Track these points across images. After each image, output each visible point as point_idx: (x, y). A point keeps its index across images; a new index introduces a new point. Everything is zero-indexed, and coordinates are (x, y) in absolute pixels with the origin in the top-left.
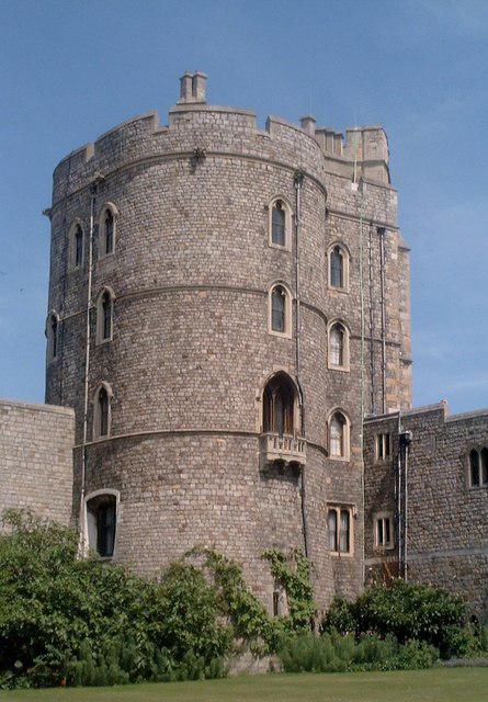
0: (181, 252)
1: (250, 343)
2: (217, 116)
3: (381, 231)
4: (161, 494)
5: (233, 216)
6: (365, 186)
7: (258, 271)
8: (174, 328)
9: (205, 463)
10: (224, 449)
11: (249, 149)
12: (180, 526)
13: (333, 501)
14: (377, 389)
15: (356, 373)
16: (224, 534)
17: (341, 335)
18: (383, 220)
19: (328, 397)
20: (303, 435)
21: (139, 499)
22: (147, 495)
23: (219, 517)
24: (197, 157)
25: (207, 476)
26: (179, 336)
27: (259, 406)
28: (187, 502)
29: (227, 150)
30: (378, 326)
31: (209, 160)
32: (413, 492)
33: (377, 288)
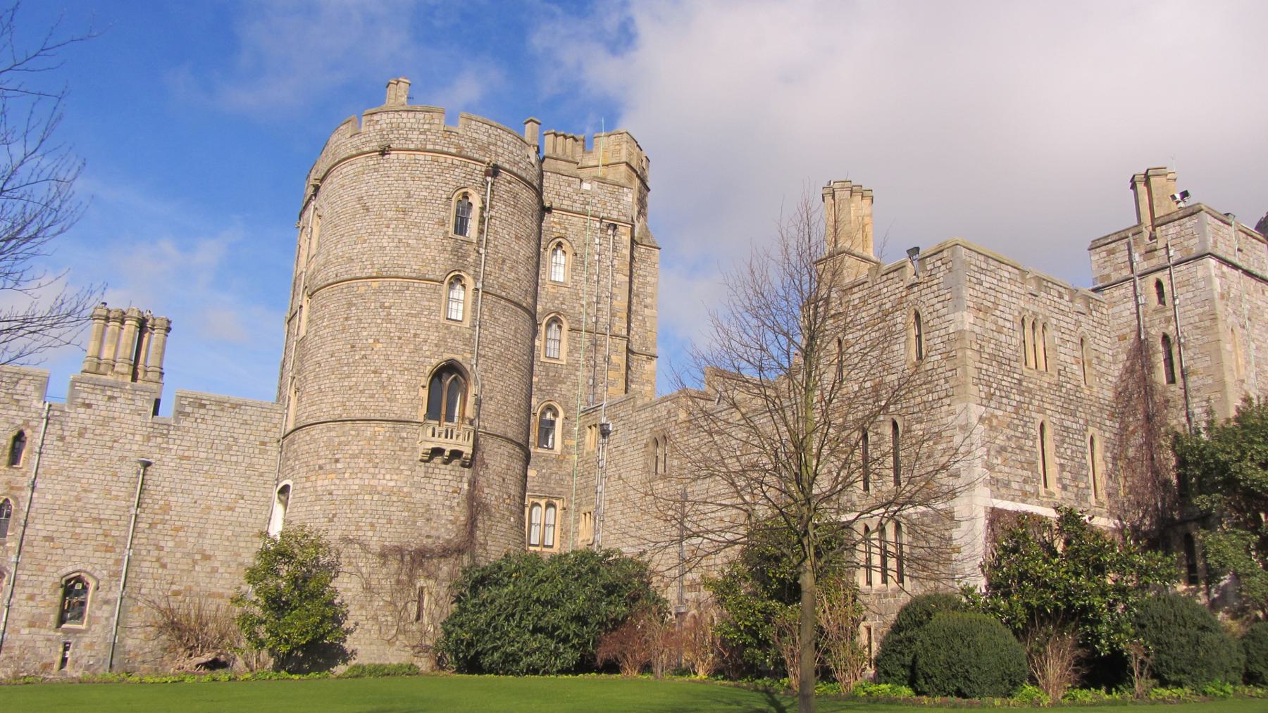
0: (359, 246)
1: (419, 332)
2: (404, 115)
7: (435, 260)
8: (347, 319)
10: (381, 437)
11: (435, 143)
12: (331, 516)
13: (537, 494)
15: (574, 367)
16: (372, 525)
22: (309, 484)
23: (368, 508)
25: (362, 465)
27: (424, 394)
29: (412, 146)
31: (393, 155)
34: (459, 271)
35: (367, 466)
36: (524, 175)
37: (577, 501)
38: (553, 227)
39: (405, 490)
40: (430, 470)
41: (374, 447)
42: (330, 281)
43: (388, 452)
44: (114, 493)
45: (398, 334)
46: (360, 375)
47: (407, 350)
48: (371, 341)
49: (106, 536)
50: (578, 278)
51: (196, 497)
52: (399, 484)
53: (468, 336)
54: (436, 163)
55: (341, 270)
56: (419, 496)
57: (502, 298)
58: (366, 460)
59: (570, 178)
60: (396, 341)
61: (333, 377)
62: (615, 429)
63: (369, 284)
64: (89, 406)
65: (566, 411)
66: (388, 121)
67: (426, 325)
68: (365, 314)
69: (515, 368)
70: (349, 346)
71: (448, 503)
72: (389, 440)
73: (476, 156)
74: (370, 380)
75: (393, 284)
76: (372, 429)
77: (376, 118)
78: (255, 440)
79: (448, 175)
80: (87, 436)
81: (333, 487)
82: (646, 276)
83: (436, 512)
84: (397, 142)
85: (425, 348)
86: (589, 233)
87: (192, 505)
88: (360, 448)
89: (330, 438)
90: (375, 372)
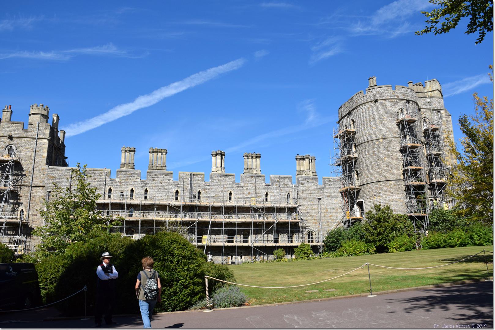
0: (374, 130)
2: (380, 89)
3: (439, 112)
5: (388, 117)
8: (374, 152)
10: (392, 185)
11: (390, 96)
18: (439, 108)
22: (371, 200)
24: (376, 101)
25: (388, 193)
29: (384, 98)
31: (379, 102)
39: (402, 199)
48: (384, 157)
52: (400, 198)
64: (303, 184)
73: (403, 98)
80: (304, 192)
89: (376, 187)
90: (386, 167)
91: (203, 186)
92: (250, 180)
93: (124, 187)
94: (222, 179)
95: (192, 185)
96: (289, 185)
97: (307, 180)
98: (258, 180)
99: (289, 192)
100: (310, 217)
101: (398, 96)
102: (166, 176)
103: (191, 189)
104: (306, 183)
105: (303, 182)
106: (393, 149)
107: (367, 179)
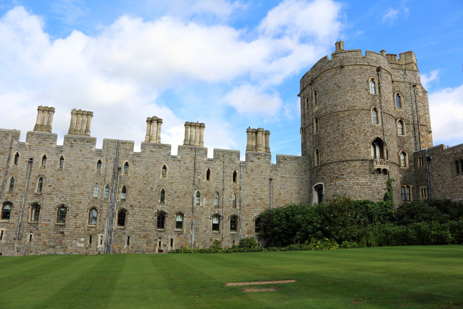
0: (339, 100)
1: (365, 128)
2: (348, 53)
3: (414, 86)
4: (337, 183)
5: (356, 86)
6: (407, 71)
7: (367, 103)
8: (338, 126)
9: (351, 171)
12: (344, 194)
14: (418, 141)
17: (402, 124)
18: (415, 82)
19: (399, 146)
20: (388, 159)
21: (330, 185)
22: (332, 183)
23: (358, 190)
24: (342, 67)
25: (353, 176)
26: (340, 128)
28: (346, 185)
29: (352, 64)
30: (416, 120)
31: (346, 68)
32: (433, 178)
33: (415, 106)
34: (375, 106)
35: (355, 176)
36: (388, 70)
37: (417, 185)
38: (395, 88)
39: (369, 183)
40: (376, 176)
41: (356, 169)
42: (328, 113)
43: (361, 171)
44: (264, 190)
45: (358, 130)
46: (347, 145)
47: (362, 135)
48: (349, 133)
49: (264, 204)
50: (406, 105)
51: (288, 190)
52: (367, 181)
53: (381, 129)
54: (361, 69)
55: (333, 109)
56: (374, 185)
57: (388, 114)
58: (354, 174)
59: (398, 70)
60: (358, 132)
61: (336, 146)
62: (433, 158)
63: (345, 113)
64: (252, 161)
65: (408, 153)
66: (342, 56)
67: (367, 126)
68: (345, 124)
69: (395, 139)
70: (341, 135)
71: (383, 187)
72: (361, 167)
73: (374, 65)
74: (351, 146)
75: (354, 112)
76: (354, 163)
77: (337, 55)
78: (303, 170)
79: (366, 73)
80: (254, 171)
81: (343, 184)
82: (424, 103)
83: (380, 190)
84: (347, 63)
85: (368, 134)
86: (407, 89)
87: (287, 193)
88: (351, 170)
90: (352, 143)
91: (132, 157)
92: (189, 153)
93: (35, 152)
94: (155, 150)
95: (118, 153)
96: (235, 162)
97: (258, 157)
98: (199, 154)
99: (235, 170)
100: (259, 201)
101: (369, 63)
102: (87, 142)
103: (116, 160)
104: (256, 160)
105: (253, 158)
106: (360, 123)
107: (328, 158)
